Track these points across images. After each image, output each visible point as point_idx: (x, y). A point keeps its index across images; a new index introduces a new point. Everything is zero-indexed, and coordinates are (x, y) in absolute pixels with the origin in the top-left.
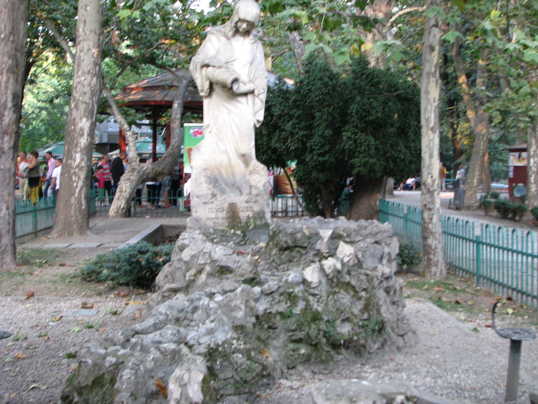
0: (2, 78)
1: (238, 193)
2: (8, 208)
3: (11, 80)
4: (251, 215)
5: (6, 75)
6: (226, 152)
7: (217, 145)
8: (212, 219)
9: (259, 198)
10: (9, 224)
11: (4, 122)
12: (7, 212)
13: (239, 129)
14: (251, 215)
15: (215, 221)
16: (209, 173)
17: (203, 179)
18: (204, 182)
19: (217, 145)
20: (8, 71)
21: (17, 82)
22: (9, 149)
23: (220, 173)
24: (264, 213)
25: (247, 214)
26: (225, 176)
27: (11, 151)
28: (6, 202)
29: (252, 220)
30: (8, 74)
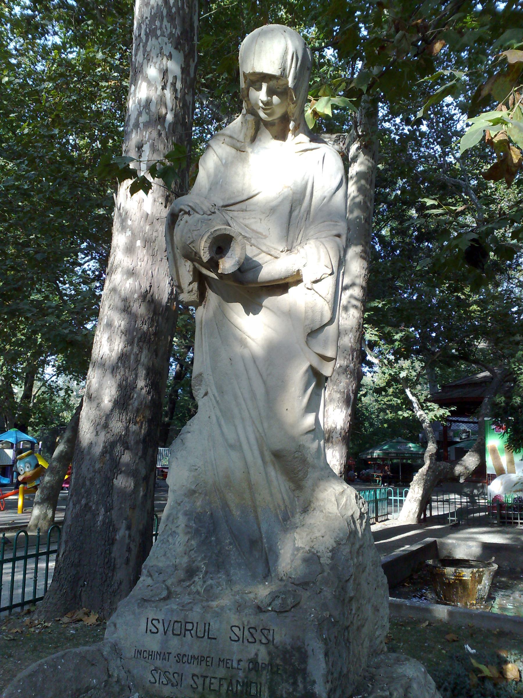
0: (132, 349)
1: (260, 569)
2: (129, 528)
3: (145, 352)
4: (263, 656)
5: (138, 345)
6: (236, 447)
7: (220, 425)
8: (151, 654)
9: (305, 595)
10: (129, 550)
11: (131, 407)
12: (127, 532)
13: (264, 382)
14: (263, 656)
15: (158, 663)
16: (199, 503)
17: (182, 521)
18: (180, 530)
19: (220, 425)
20: (140, 340)
21: (157, 355)
22: (137, 443)
23: (225, 505)
24: (304, 657)
25: (252, 649)
26: (236, 513)
27: (141, 446)
28: (126, 519)
29: (265, 676)
30: (141, 344)
